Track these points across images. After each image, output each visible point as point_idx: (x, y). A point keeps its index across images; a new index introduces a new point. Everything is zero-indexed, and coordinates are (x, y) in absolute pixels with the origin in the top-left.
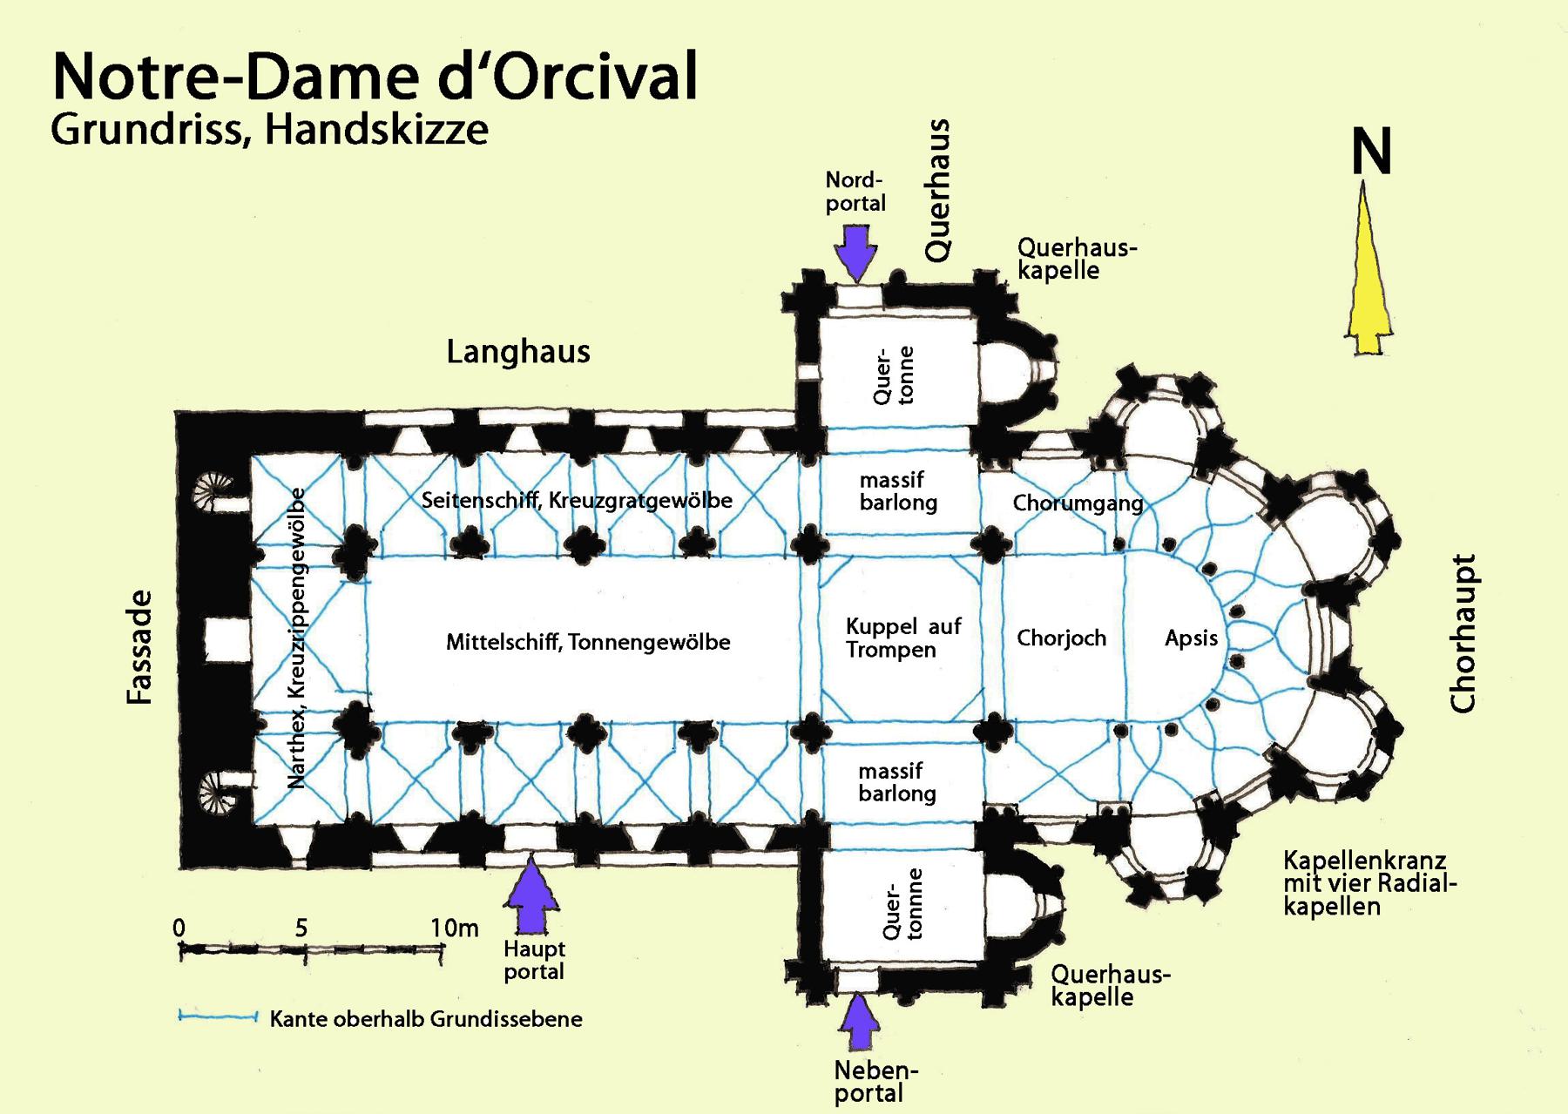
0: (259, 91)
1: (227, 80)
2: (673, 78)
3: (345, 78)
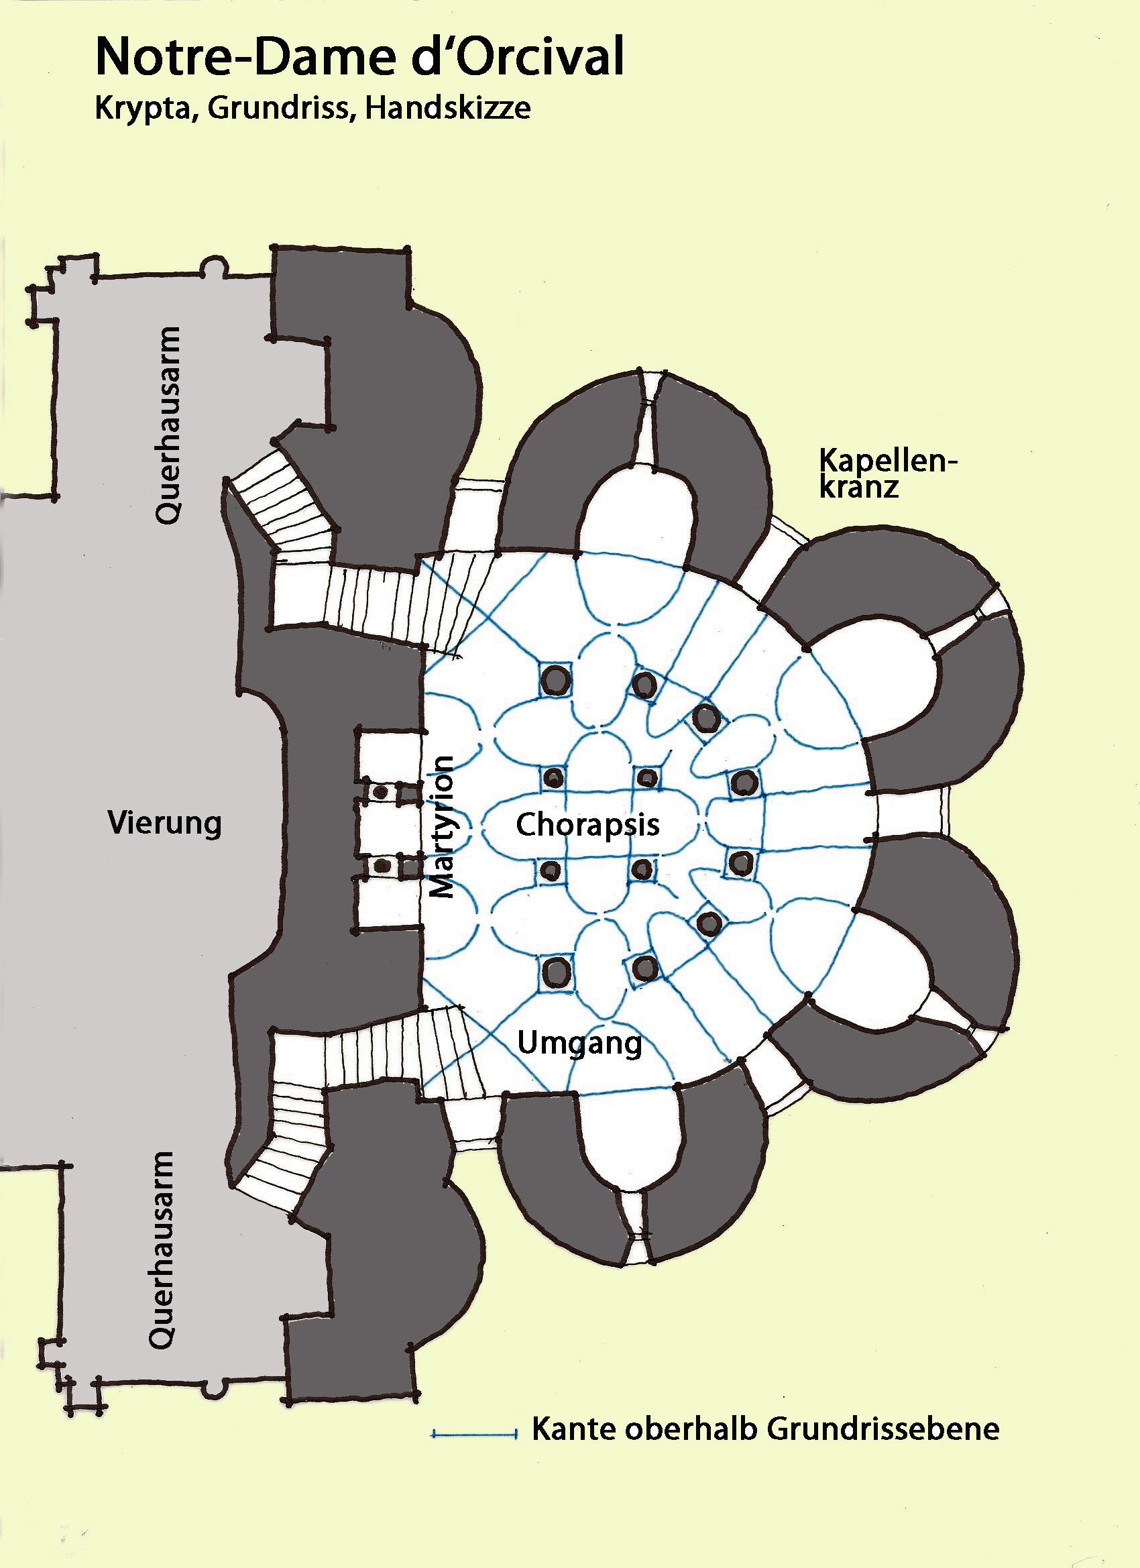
0: (265, 68)
1: (238, 59)
2: (604, 58)
3: (336, 57)
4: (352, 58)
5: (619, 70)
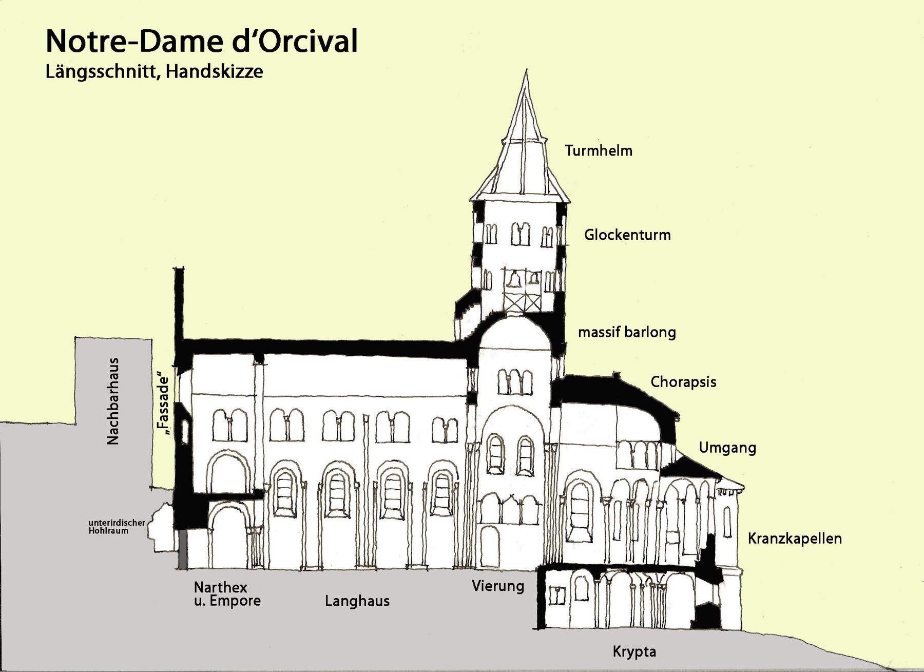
0: (146, 48)
1: (130, 43)
3: (188, 42)
4: (197, 42)
5: (355, 49)
